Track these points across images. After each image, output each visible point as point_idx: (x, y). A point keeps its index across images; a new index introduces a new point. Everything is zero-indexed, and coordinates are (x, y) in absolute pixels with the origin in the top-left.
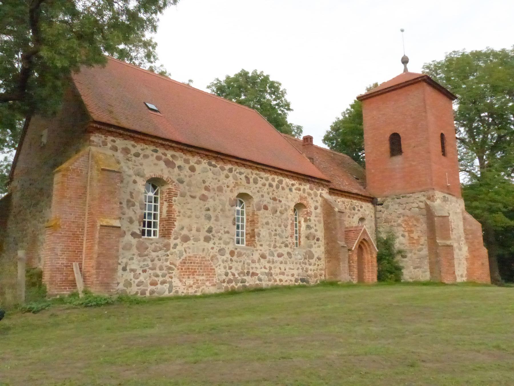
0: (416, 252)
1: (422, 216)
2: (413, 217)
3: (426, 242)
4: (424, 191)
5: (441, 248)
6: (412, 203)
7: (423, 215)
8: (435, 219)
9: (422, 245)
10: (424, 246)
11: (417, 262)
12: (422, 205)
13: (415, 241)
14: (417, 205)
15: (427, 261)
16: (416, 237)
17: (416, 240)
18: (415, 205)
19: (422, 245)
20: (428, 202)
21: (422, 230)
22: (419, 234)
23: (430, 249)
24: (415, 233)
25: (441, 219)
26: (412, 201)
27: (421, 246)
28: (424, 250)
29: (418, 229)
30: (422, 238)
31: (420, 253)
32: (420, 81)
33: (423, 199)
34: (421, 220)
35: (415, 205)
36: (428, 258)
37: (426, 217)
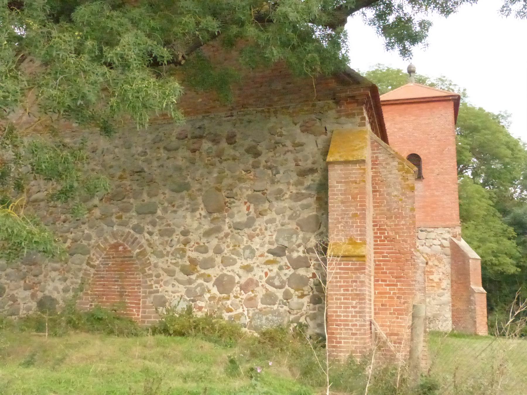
0: (436, 297)
1: (445, 257)
2: (435, 255)
3: (449, 286)
4: (449, 228)
5: (476, 295)
6: (433, 239)
7: (446, 255)
8: (470, 261)
9: (444, 289)
10: (446, 291)
11: (437, 309)
12: (446, 243)
13: (434, 285)
14: (439, 243)
15: (449, 307)
16: (436, 280)
17: (436, 283)
18: (436, 242)
19: (444, 289)
20: (455, 240)
21: (445, 272)
22: (441, 276)
23: (455, 295)
24: (435, 274)
25: (474, 261)
26: (434, 237)
27: (442, 291)
28: (446, 295)
29: (440, 270)
30: (444, 281)
31: (441, 298)
32: (449, 100)
33: (447, 236)
34: (444, 260)
35: (436, 242)
36: (450, 304)
37: (450, 257)
